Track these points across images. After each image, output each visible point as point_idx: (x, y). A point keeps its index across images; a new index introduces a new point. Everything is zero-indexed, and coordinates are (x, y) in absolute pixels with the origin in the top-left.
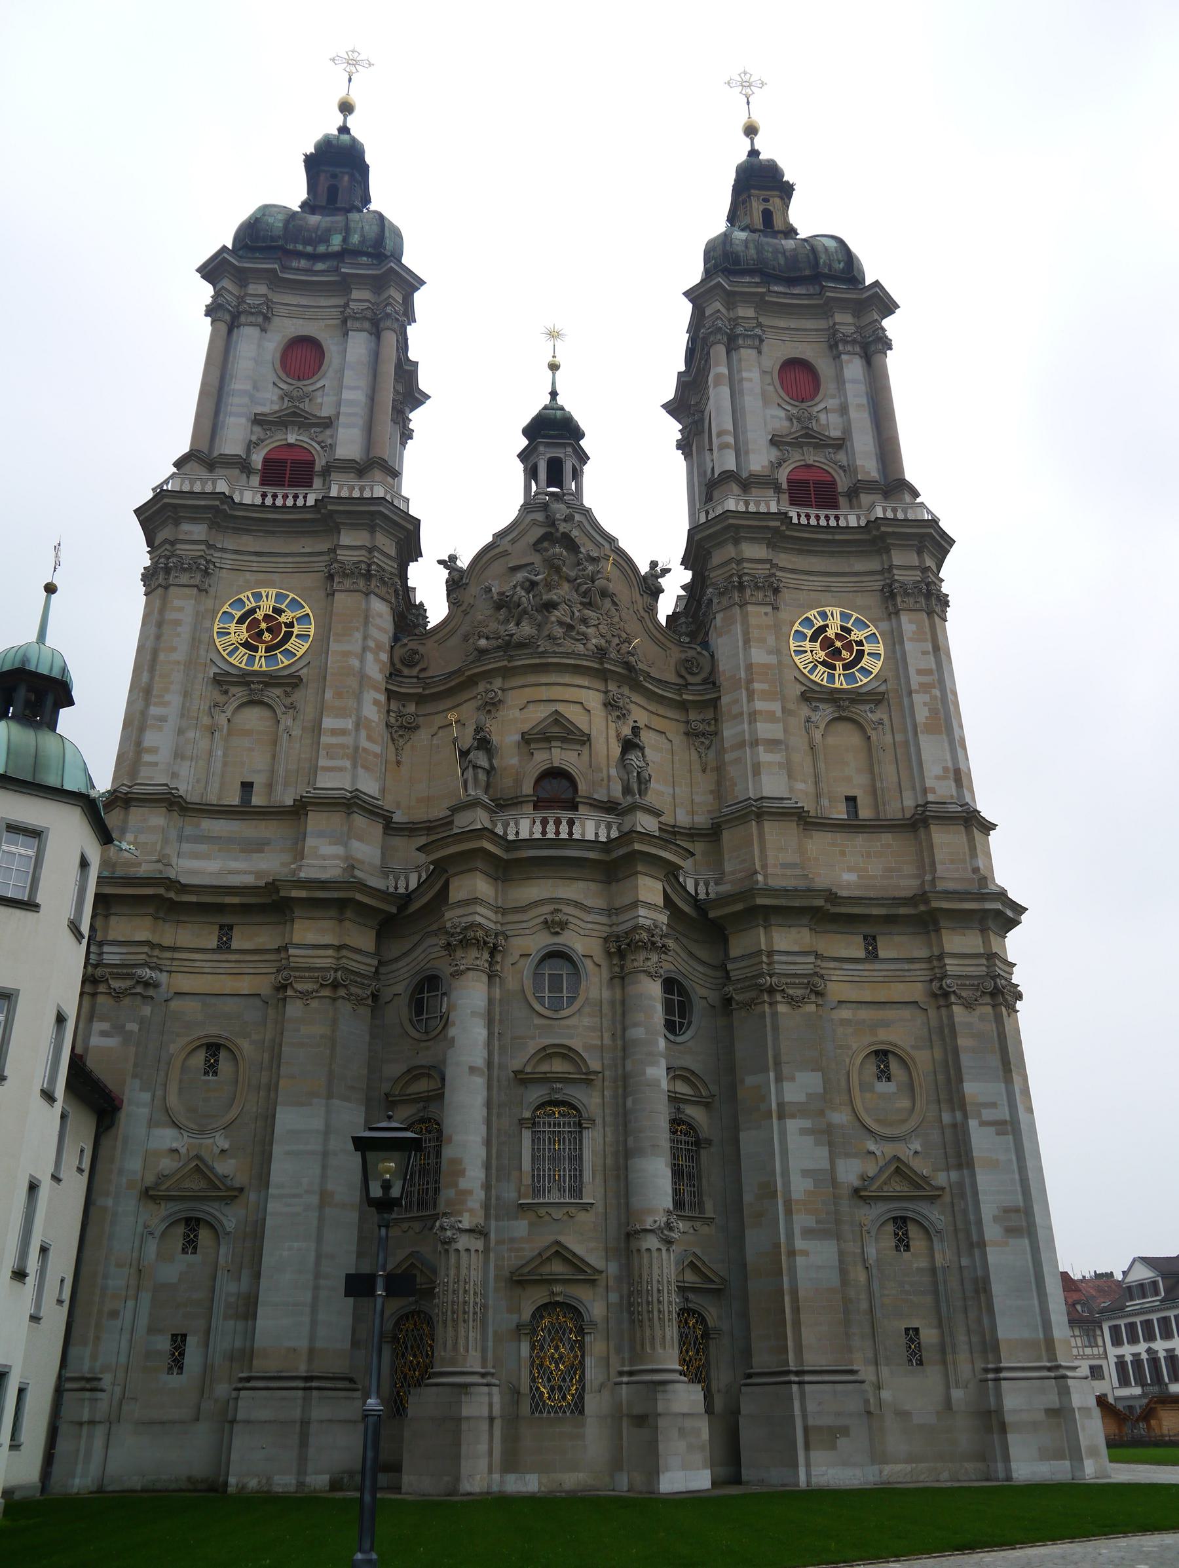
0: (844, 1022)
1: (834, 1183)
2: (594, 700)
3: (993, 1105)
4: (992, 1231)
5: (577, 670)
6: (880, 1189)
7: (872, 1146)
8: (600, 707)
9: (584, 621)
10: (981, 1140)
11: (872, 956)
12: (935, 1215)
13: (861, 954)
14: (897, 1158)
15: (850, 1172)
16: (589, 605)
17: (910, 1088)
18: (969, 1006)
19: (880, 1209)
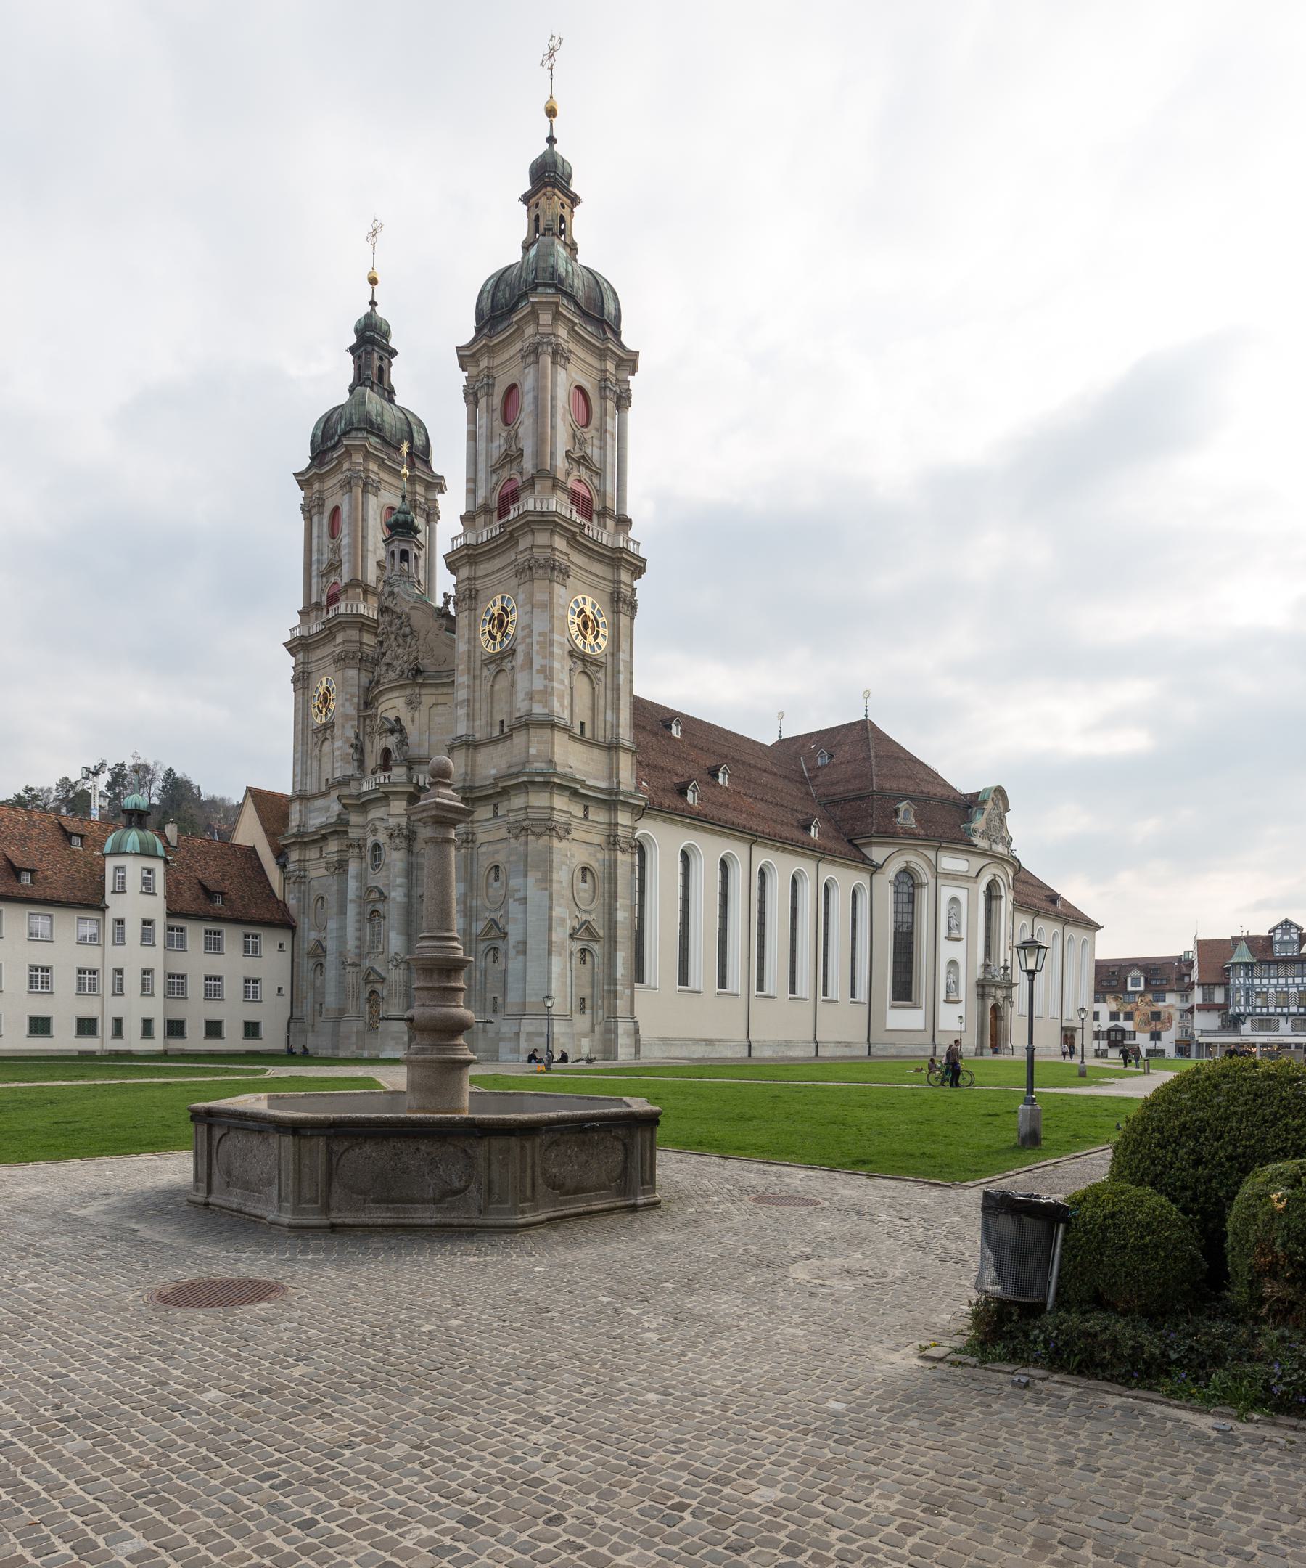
0: (484, 853)
1: (471, 934)
2: (400, 702)
3: (519, 890)
4: (512, 953)
5: (392, 689)
6: (486, 934)
7: (487, 915)
8: (404, 705)
9: (397, 657)
10: (513, 907)
11: (496, 814)
12: (500, 944)
13: (491, 815)
14: (493, 920)
15: (478, 927)
16: (399, 645)
17: (502, 884)
18: (517, 837)
19: (487, 943)
